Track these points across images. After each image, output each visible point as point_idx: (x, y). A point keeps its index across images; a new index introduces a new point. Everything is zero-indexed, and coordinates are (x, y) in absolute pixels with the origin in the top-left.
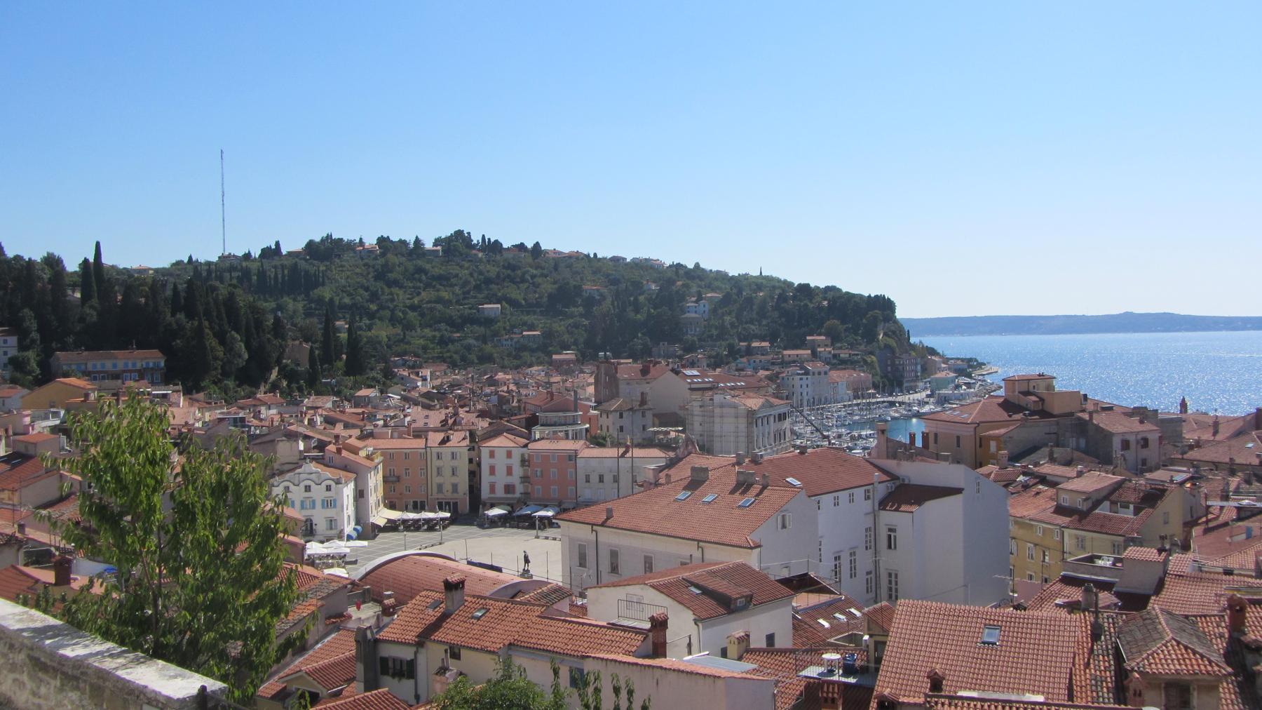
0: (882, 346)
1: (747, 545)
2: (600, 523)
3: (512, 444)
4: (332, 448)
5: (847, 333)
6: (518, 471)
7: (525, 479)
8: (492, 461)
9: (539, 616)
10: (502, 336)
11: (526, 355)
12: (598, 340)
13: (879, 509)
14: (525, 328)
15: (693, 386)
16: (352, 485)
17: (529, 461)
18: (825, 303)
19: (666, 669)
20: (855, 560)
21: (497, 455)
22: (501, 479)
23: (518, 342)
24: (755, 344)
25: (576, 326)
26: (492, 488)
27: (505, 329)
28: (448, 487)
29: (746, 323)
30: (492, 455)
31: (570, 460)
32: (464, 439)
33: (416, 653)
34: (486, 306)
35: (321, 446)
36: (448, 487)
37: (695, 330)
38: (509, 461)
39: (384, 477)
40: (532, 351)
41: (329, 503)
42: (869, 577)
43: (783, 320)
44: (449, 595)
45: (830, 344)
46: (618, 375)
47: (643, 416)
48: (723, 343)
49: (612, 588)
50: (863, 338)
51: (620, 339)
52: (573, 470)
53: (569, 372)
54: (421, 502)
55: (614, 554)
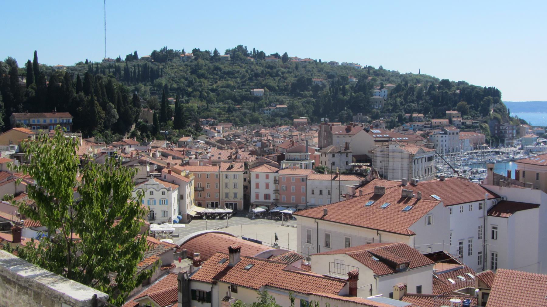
0: (492, 117)
1: (406, 233)
2: (320, 217)
3: (270, 171)
4: (165, 170)
5: (471, 110)
6: (272, 187)
7: (276, 191)
8: (257, 180)
9: (283, 270)
10: (264, 107)
11: (278, 120)
12: (321, 110)
13: (488, 215)
14: (278, 103)
15: (377, 139)
16: (176, 192)
17: (278, 181)
18: (458, 91)
19: (357, 303)
20: (471, 244)
21: (260, 176)
22: (262, 191)
23: (274, 111)
24: (415, 115)
25: (308, 102)
26: (257, 196)
27: (266, 103)
28: (231, 195)
29: (410, 102)
30: (257, 176)
32: (241, 167)
33: (212, 288)
34: (255, 90)
35: (160, 169)
36: (231, 195)
37: (379, 107)
38: (267, 181)
39: (195, 188)
40: (282, 117)
41: (164, 202)
42: (480, 255)
43: (432, 101)
44: (231, 255)
46: (332, 132)
47: (347, 156)
49: (326, 256)
50: (480, 113)
51: (334, 111)
52: (305, 187)
53: (303, 130)
54: (216, 203)
55: (328, 236)
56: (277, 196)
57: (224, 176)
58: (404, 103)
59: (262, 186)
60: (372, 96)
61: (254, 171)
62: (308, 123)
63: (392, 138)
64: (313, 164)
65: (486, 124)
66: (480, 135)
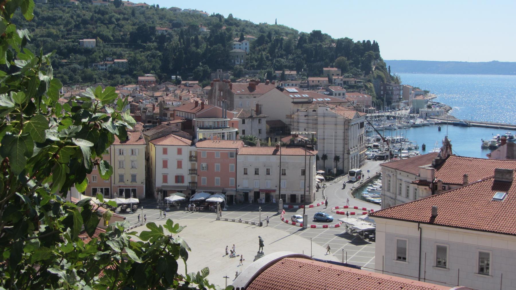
0: (376, 76)
5: (351, 67)
6: (187, 165)
7: (193, 171)
10: (98, 62)
12: (171, 66)
14: (114, 57)
15: (295, 100)
17: (196, 157)
21: (169, 151)
22: (172, 171)
23: (111, 67)
24: (287, 72)
25: (153, 56)
26: (165, 178)
27: (100, 57)
28: (128, 178)
29: (278, 57)
30: (165, 151)
31: (232, 156)
32: (140, 138)
36: (128, 178)
37: (241, 62)
38: (179, 157)
40: (122, 74)
43: (305, 55)
45: (340, 74)
48: (263, 71)
50: (362, 70)
52: (234, 165)
54: (105, 189)
55: (441, 250)
56: (193, 178)
57: (117, 152)
58: (270, 58)
60: (232, 49)
61: (160, 143)
62: (157, 81)
64: (237, 133)
65: (371, 84)
66: (366, 96)
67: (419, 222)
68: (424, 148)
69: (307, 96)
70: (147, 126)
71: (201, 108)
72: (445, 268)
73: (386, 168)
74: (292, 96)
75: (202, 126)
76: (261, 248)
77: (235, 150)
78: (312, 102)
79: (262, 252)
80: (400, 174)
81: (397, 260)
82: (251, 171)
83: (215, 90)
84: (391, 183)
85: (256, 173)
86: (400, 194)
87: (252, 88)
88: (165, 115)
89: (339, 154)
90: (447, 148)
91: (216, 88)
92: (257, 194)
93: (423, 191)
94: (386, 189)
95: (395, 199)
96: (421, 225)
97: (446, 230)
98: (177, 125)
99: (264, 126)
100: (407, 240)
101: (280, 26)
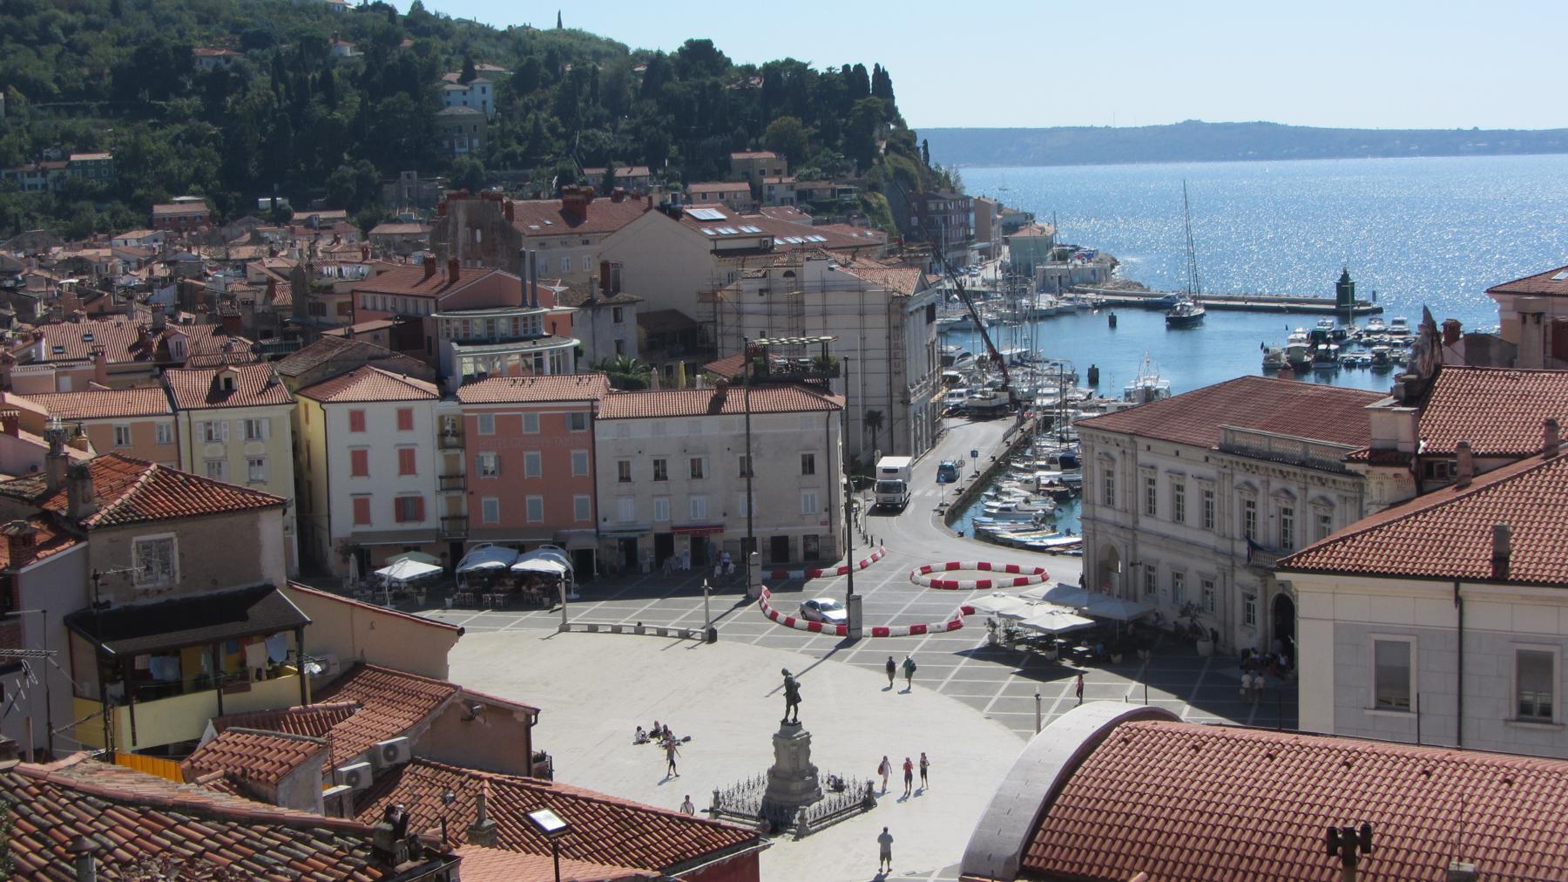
0: (890, 171)
6: (431, 462)
7: (451, 481)
10: (17, 165)
11: (90, 212)
12: (253, 169)
14: (69, 146)
15: (721, 245)
22: (385, 484)
23: (61, 177)
24: (621, 172)
25: (194, 138)
26: (362, 508)
27: (21, 149)
29: (588, 126)
30: (358, 422)
31: (578, 425)
37: (471, 146)
38: (406, 437)
40: (99, 198)
43: (671, 117)
45: (785, 170)
46: (516, 224)
47: (617, 319)
48: (545, 171)
57: (200, 433)
58: (562, 130)
59: (383, 462)
61: (341, 396)
62: (212, 217)
63: (773, 237)
64: (577, 351)
65: (881, 196)
66: (869, 233)
67: (1458, 580)
68: (1093, 378)
69: (756, 230)
70: (265, 348)
71: (447, 277)
72: (1550, 722)
73: (1095, 433)
74: (709, 232)
75: (461, 336)
76: (792, 707)
77: (588, 404)
78: (772, 247)
79: (795, 719)
80: (1149, 448)
81: (1377, 708)
82: (642, 469)
83: (456, 226)
84: (1118, 477)
85: (660, 474)
86: (1151, 511)
87: (573, 214)
88: (320, 309)
89: (878, 404)
90: (1432, 342)
91: (456, 219)
92: (664, 543)
93: (1382, 484)
94: (1098, 499)
95: (1134, 530)
96: (1464, 587)
97: (1551, 599)
98: (376, 338)
99: (631, 331)
100: (1412, 639)
101: (574, 34)
